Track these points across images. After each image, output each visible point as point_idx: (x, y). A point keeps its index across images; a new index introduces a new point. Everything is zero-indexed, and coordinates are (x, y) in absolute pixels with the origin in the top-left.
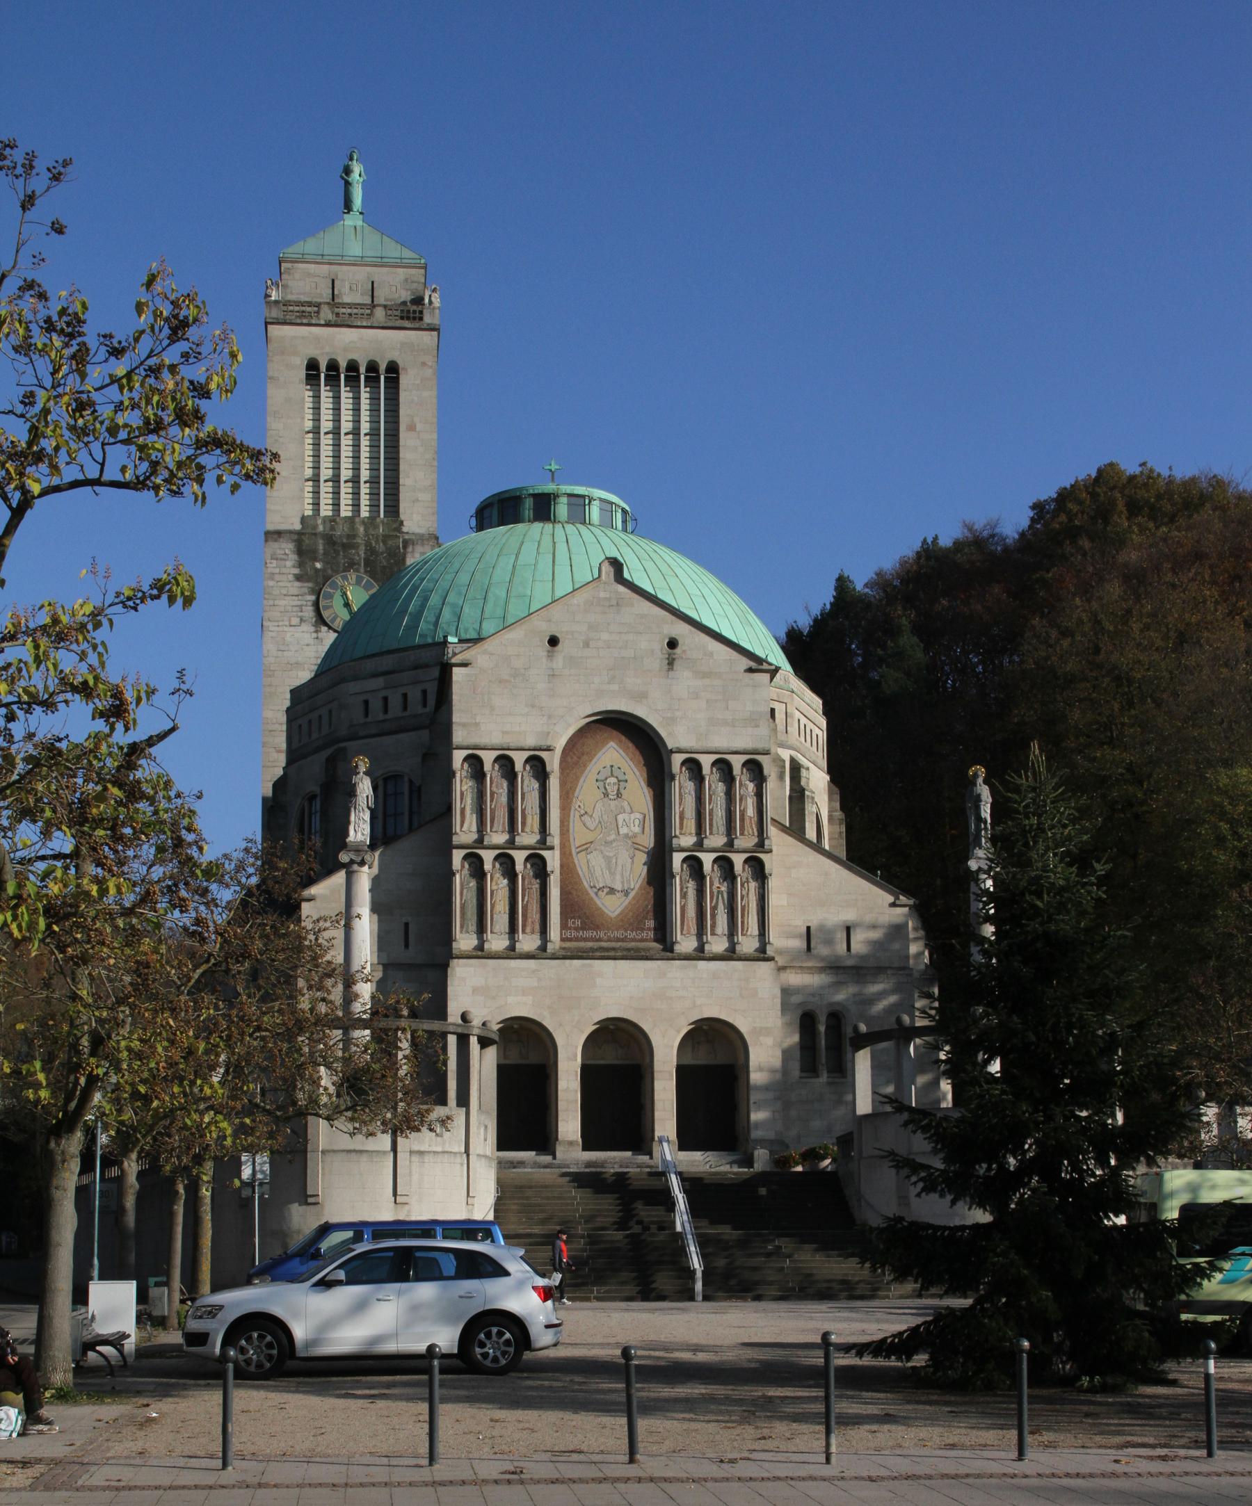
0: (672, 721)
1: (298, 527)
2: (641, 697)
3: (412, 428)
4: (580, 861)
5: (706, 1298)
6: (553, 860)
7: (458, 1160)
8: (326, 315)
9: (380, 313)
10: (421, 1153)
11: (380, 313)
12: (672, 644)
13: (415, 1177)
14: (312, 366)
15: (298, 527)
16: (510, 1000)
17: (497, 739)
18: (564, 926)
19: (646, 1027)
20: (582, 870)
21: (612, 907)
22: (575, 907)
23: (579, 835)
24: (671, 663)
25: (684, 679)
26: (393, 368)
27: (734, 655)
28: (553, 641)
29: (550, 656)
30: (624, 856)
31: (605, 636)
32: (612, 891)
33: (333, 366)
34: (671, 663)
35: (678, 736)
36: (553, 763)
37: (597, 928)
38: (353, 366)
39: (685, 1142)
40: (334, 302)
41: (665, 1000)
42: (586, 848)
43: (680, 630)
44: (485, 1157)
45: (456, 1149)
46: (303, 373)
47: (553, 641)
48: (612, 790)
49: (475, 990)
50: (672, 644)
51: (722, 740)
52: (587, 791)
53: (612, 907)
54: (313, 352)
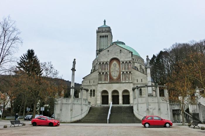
0: (121, 58)
1: (99, 49)
2: (118, 56)
3: (109, 41)
4: (111, 73)
5: (109, 123)
6: (108, 73)
7: (80, 105)
8: (101, 32)
9: (106, 31)
10: (74, 104)
11: (106, 31)
12: (121, 50)
13: (73, 107)
14: (100, 36)
15: (99, 49)
16: (104, 88)
17: (102, 61)
18: (110, 80)
19: (118, 91)
20: (112, 74)
21: (115, 78)
22: (111, 78)
23: (111, 70)
24: (121, 52)
25: (122, 54)
26: (107, 36)
27: (128, 51)
28: (108, 51)
29: (108, 52)
30: (116, 72)
31: (114, 50)
32: (115, 76)
33: (102, 36)
34: (121, 52)
35: (121, 60)
36: (108, 63)
37: (113, 80)
38: (104, 36)
39: (123, 103)
40: (102, 31)
41: (120, 88)
42: (112, 72)
43: (121, 49)
44: (85, 104)
45: (80, 103)
46: (99, 37)
47: (108, 51)
48: (115, 66)
49: (100, 87)
50: (121, 50)
51: (126, 60)
52: (112, 66)
53: (115, 78)
54: (100, 35)
